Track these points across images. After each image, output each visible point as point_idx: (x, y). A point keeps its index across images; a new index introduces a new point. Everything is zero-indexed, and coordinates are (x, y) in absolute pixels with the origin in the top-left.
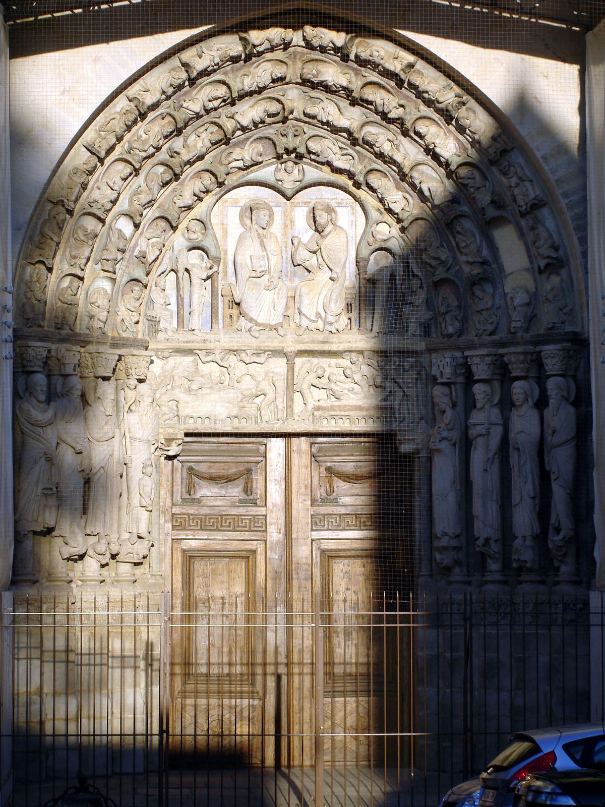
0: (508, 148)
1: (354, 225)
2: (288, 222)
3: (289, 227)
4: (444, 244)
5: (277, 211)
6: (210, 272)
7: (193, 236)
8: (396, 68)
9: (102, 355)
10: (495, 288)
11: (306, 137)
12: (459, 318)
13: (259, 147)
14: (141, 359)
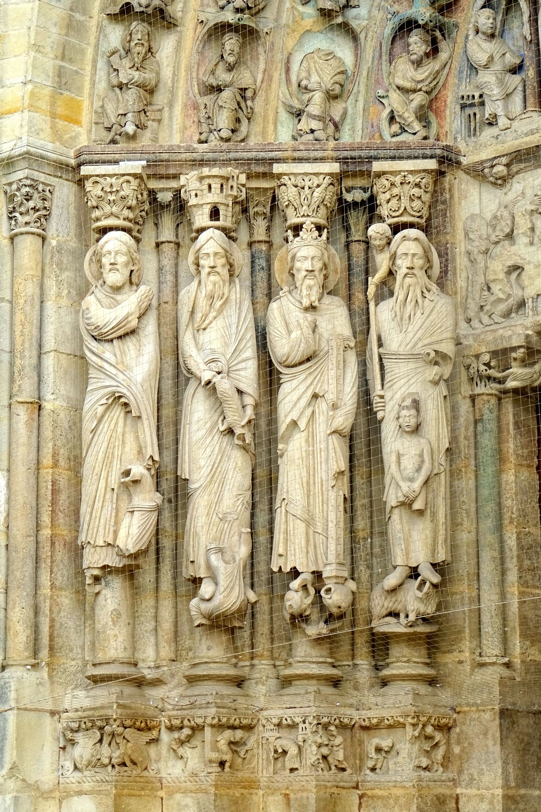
9: (285, 179)
14: (398, 179)
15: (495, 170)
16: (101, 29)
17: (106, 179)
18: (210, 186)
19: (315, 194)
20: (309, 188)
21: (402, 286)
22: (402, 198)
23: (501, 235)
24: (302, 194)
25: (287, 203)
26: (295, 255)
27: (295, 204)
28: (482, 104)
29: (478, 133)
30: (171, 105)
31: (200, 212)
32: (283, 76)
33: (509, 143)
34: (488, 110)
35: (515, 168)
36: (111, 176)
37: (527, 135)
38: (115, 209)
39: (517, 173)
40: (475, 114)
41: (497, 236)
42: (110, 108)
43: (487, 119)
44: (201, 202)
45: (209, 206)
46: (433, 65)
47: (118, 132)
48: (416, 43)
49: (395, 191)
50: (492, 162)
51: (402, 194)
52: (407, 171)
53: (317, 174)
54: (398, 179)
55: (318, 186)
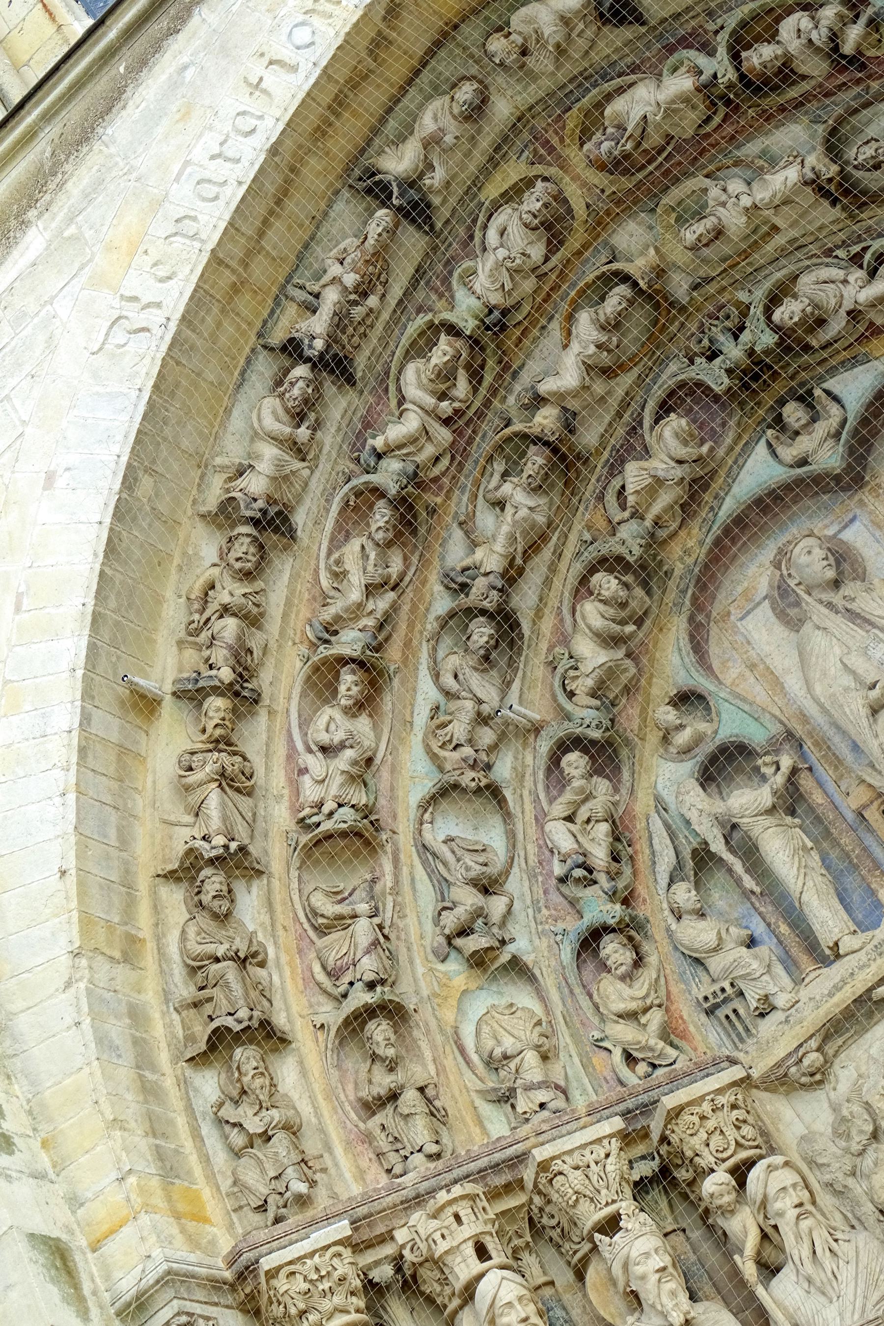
6: (779, 780)
7: (682, 738)
11: (757, 311)
13: (675, 423)
14: (706, 1107)
15: (806, 1062)
16: (184, 1083)
17: (305, 1263)
18: (457, 1217)
19: (609, 1168)
20: (597, 1163)
21: (799, 1237)
22: (724, 1130)
23: (864, 1138)
24: (590, 1175)
25: (574, 1198)
26: (628, 1257)
27: (588, 1193)
28: (741, 994)
29: (754, 1031)
30: (329, 1148)
31: (459, 1259)
32: (460, 1059)
33: (810, 1019)
34: (753, 997)
35: (830, 1049)
36: (312, 1255)
37: (831, 995)
38: (338, 1300)
39: (835, 1055)
40: (735, 1011)
41: (858, 1143)
42: (251, 1176)
43: (757, 1008)
44: (455, 1244)
45: (470, 1244)
46: (647, 975)
47: (281, 1203)
48: (616, 952)
49: (711, 1124)
50: (797, 1055)
51: (722, 1124)
52: (713, 1092)
53: (599, 1141)
54: (706, 1107)
55: (607, 1156)
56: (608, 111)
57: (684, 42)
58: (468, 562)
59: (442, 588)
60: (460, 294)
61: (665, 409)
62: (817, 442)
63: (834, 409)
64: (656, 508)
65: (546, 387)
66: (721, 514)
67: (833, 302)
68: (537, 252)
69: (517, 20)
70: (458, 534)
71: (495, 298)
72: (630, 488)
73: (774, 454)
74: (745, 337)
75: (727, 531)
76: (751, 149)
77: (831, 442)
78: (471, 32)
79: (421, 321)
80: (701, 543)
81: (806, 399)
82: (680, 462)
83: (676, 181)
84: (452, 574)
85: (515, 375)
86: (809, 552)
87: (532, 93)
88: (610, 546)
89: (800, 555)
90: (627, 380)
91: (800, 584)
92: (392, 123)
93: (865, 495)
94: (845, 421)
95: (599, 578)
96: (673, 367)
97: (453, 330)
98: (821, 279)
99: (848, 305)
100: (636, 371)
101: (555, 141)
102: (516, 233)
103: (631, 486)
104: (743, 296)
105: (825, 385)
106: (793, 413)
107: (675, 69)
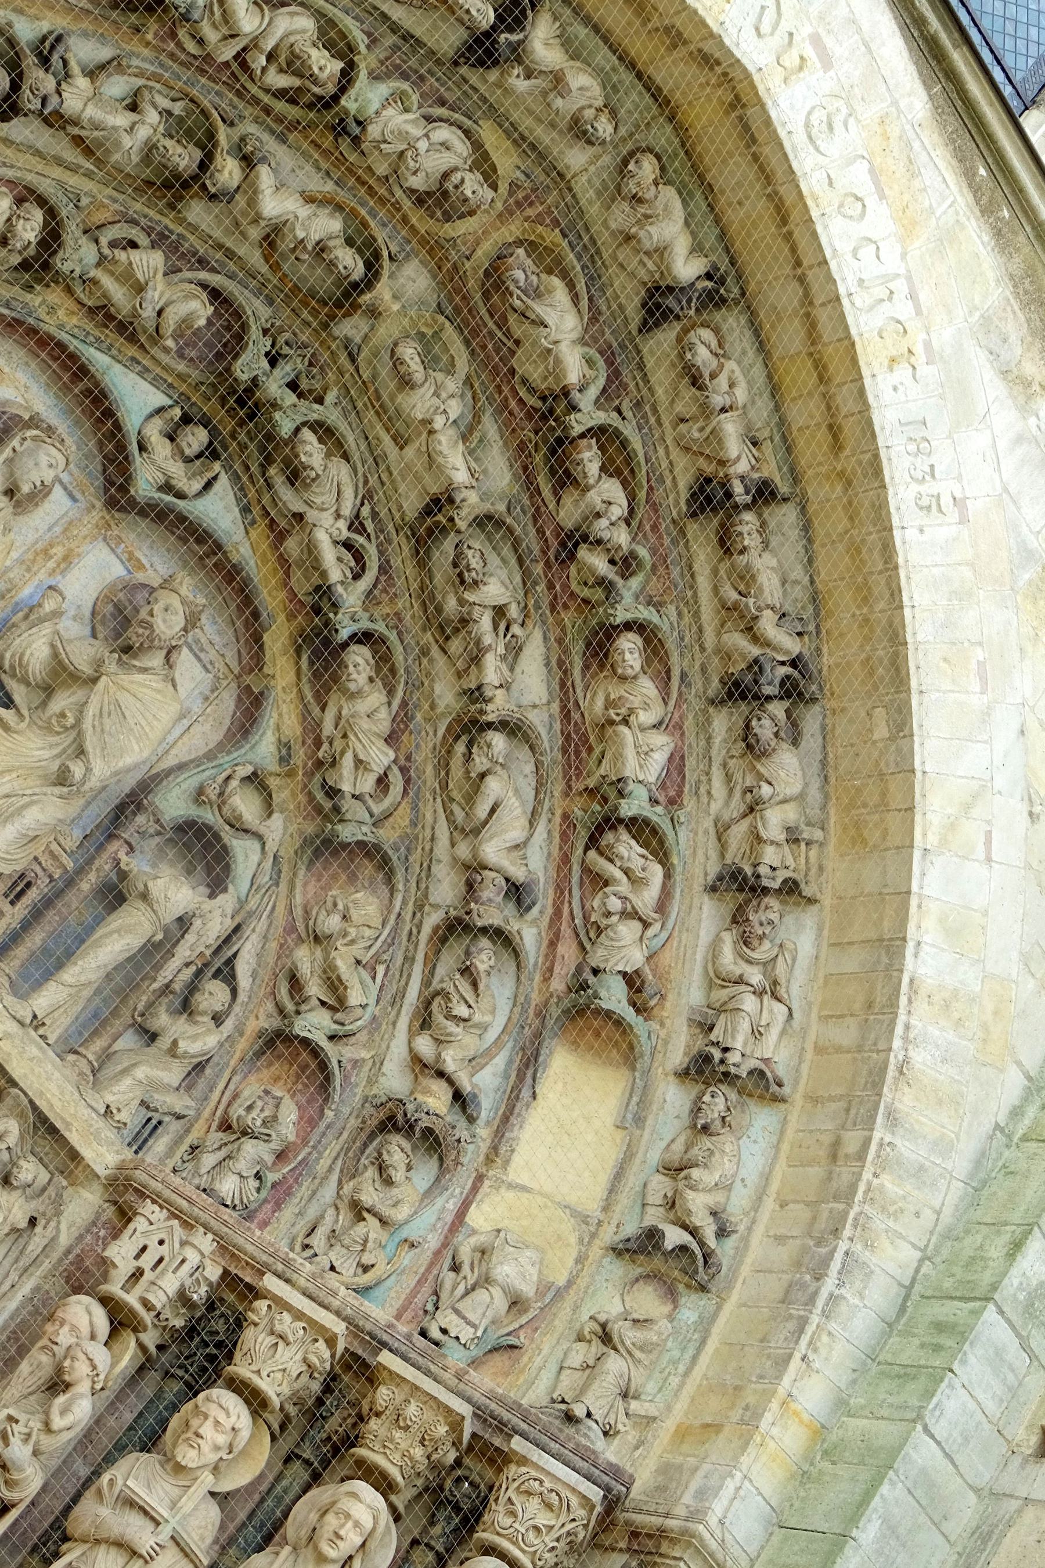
0: (807, 891)
1: (186, 722)
2: (58, 551)
3: (51, 564)
4: (381, 970)
5: (58, 503)
8: (739, 458)
10: (437, 1185)
11: (316, 413)
12: (271, 1177)
13: (201, 310)
56: (556, 282)
57: (614, 375)
58: (75, 68)
59: (45, 31)
60: (383, 89)
61: (215, 294)
62: (163, 465)
63: (197, 485)
64: (108, 282)
65: (265, 176)
66: (92, 350)
67: (318, 500)
68: (416, 182)
69: (669, 194)
70: (105, 53)
71: (374, 131)
72: (135, 255)
73: (151, 416)
74: (291, 398)
75: (73, 357)
76: (490, 426)
77: (161, 480)
78: (662, 136)
79: (360, 39)
80: (61, 327)
81: (210, 452)
82: (160, 313)
83: (467, 343)
84: (60, 49)
85: (282, 139)
86: (51, 466)
87: (586, 191)
88: (72, 232)
89: (49, 455)
90: (255, 258)
91: (14, 450)
92: (582, 32)
93: (98, 514)
94: (181, 495)
95: (38, 216)
96: (264, 312)
97: (347, 78)
98: (343, 488)
99: (311, 515)
100: (264, 269)
101: (531, 212)
102: (443, 161)
103: (138, 258)
104: (330, 398)
105: (223, 474)
106: (196, 438)
107: (590, 362)
